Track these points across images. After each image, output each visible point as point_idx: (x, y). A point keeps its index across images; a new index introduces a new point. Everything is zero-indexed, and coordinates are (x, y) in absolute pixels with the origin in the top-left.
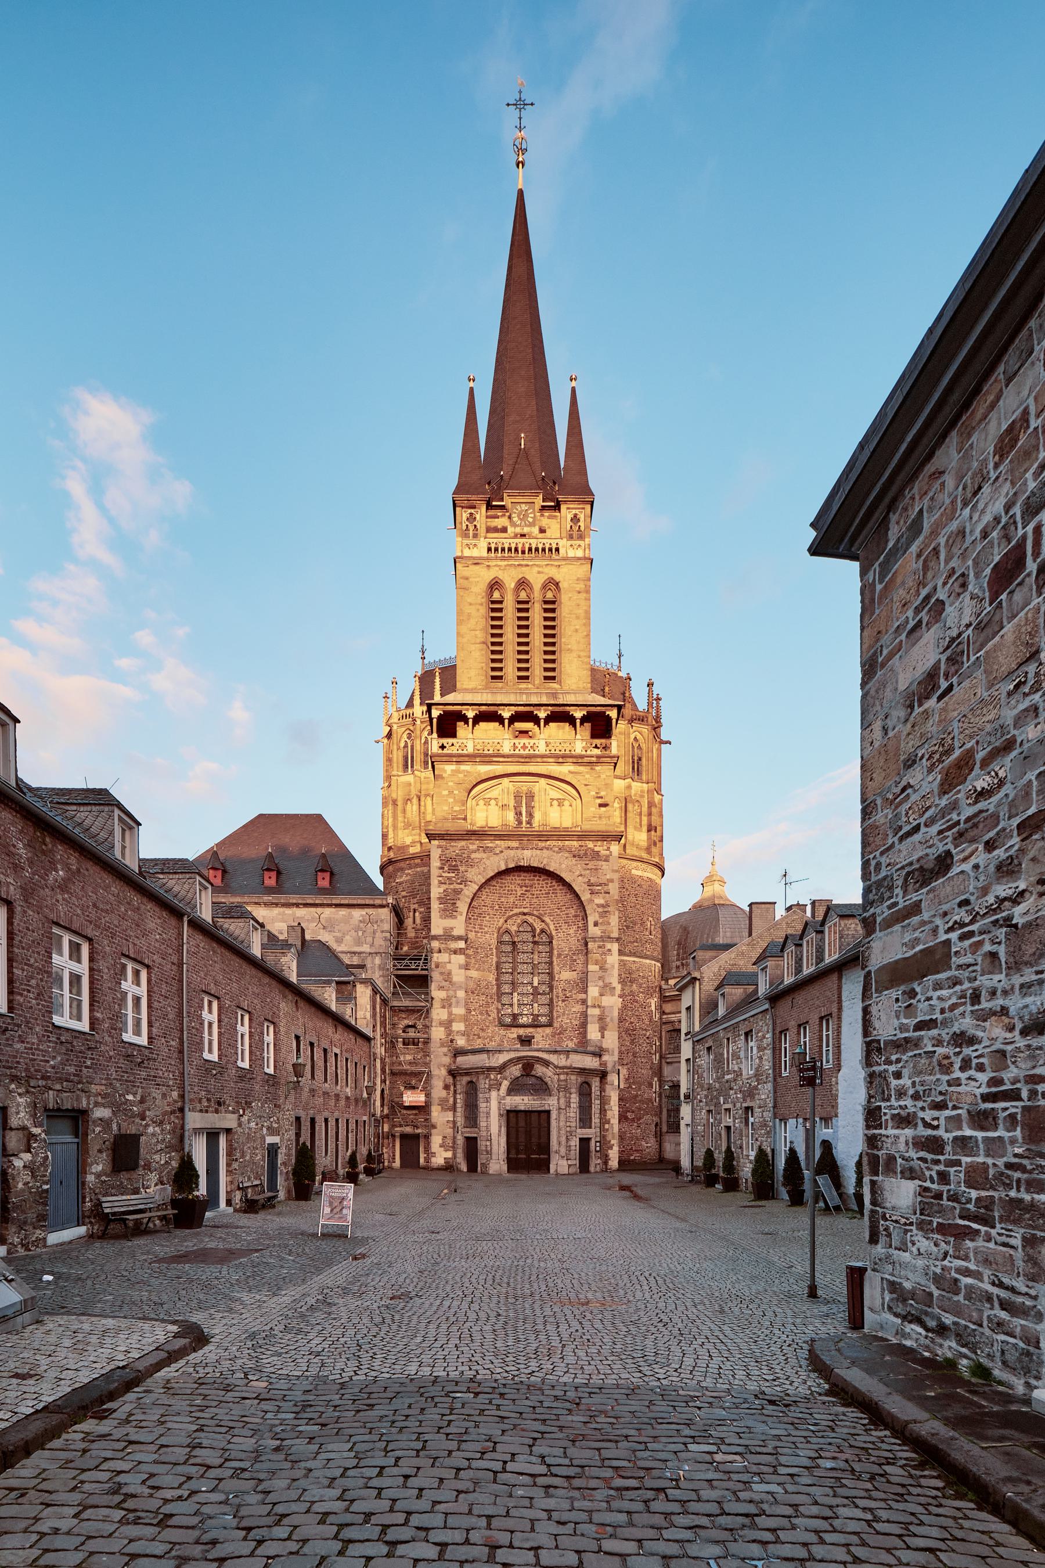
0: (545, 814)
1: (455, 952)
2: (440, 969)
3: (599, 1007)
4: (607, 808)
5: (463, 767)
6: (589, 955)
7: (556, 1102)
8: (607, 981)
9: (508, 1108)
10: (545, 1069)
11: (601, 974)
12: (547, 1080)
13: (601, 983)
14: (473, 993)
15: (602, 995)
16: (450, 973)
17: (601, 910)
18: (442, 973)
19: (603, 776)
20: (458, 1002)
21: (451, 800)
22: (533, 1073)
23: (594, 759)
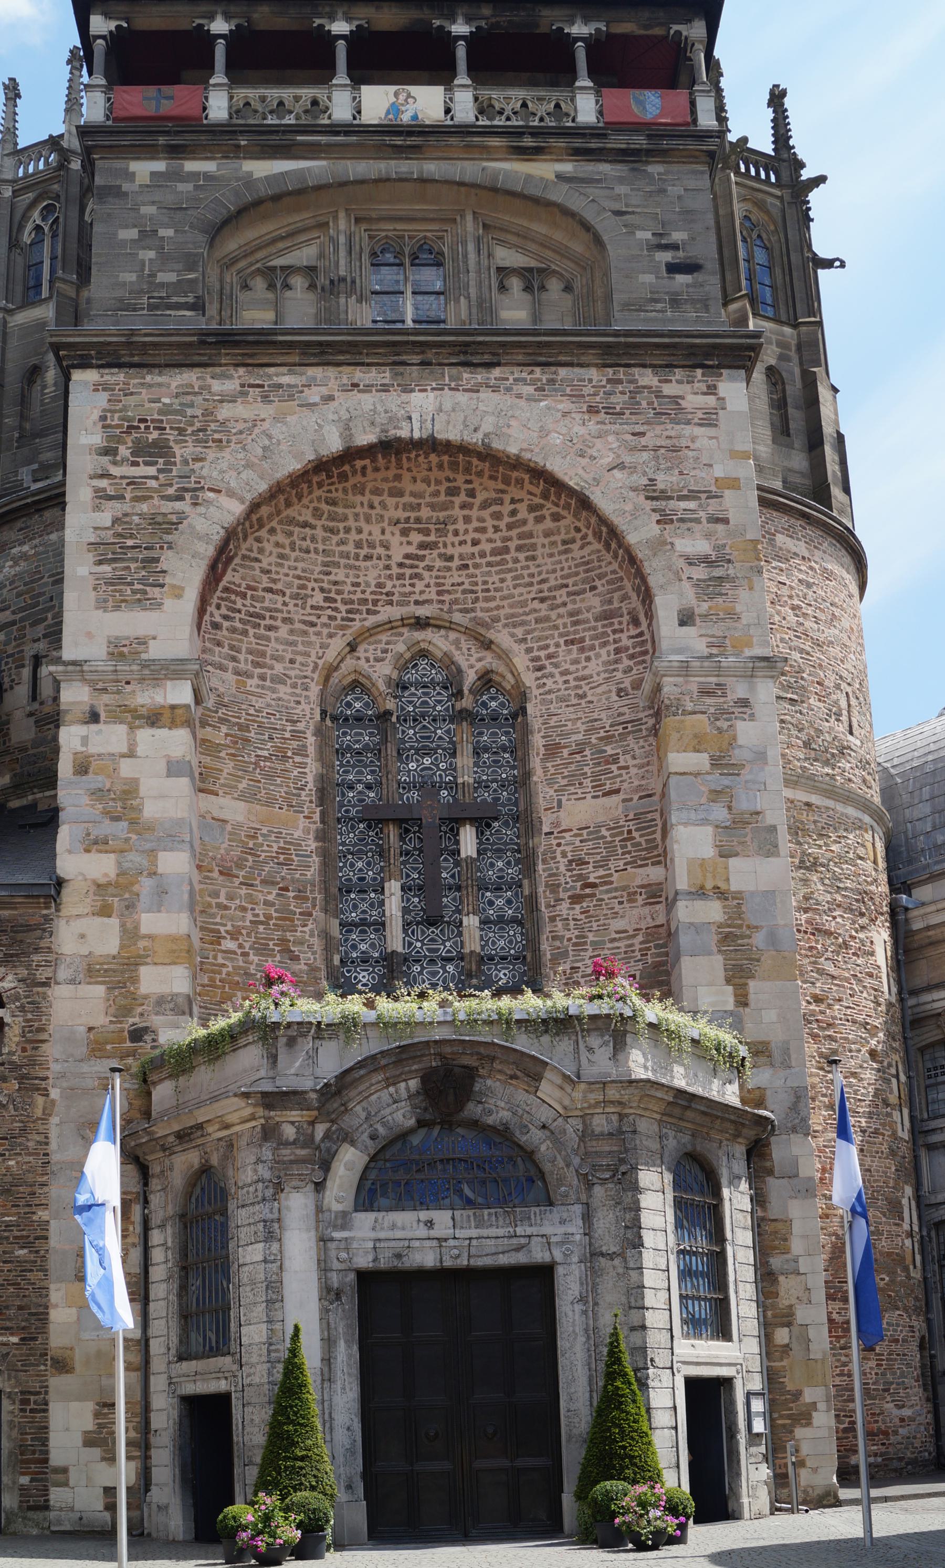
0: (485, 307)
1: (154, 718)
2: (94, 780)
3: (721, 894)
4: (699, 277)
5: (191, 166)
6: (669, 722)
7: (575, 1228)
8: (743, 804)
9: (364, 1261)
10: (521, 1096)
11: (717, 780)
12: (535, 1138)
13: (720, 813)
14: (226, 873)
15: (725, 854)
16: (130, 791)
17: (700, 573)
18: (98, 794)
19: (674, 190)
20: (161, 892)
21: (152, 254)
22: (472, 1110)
23: (640, 141)
